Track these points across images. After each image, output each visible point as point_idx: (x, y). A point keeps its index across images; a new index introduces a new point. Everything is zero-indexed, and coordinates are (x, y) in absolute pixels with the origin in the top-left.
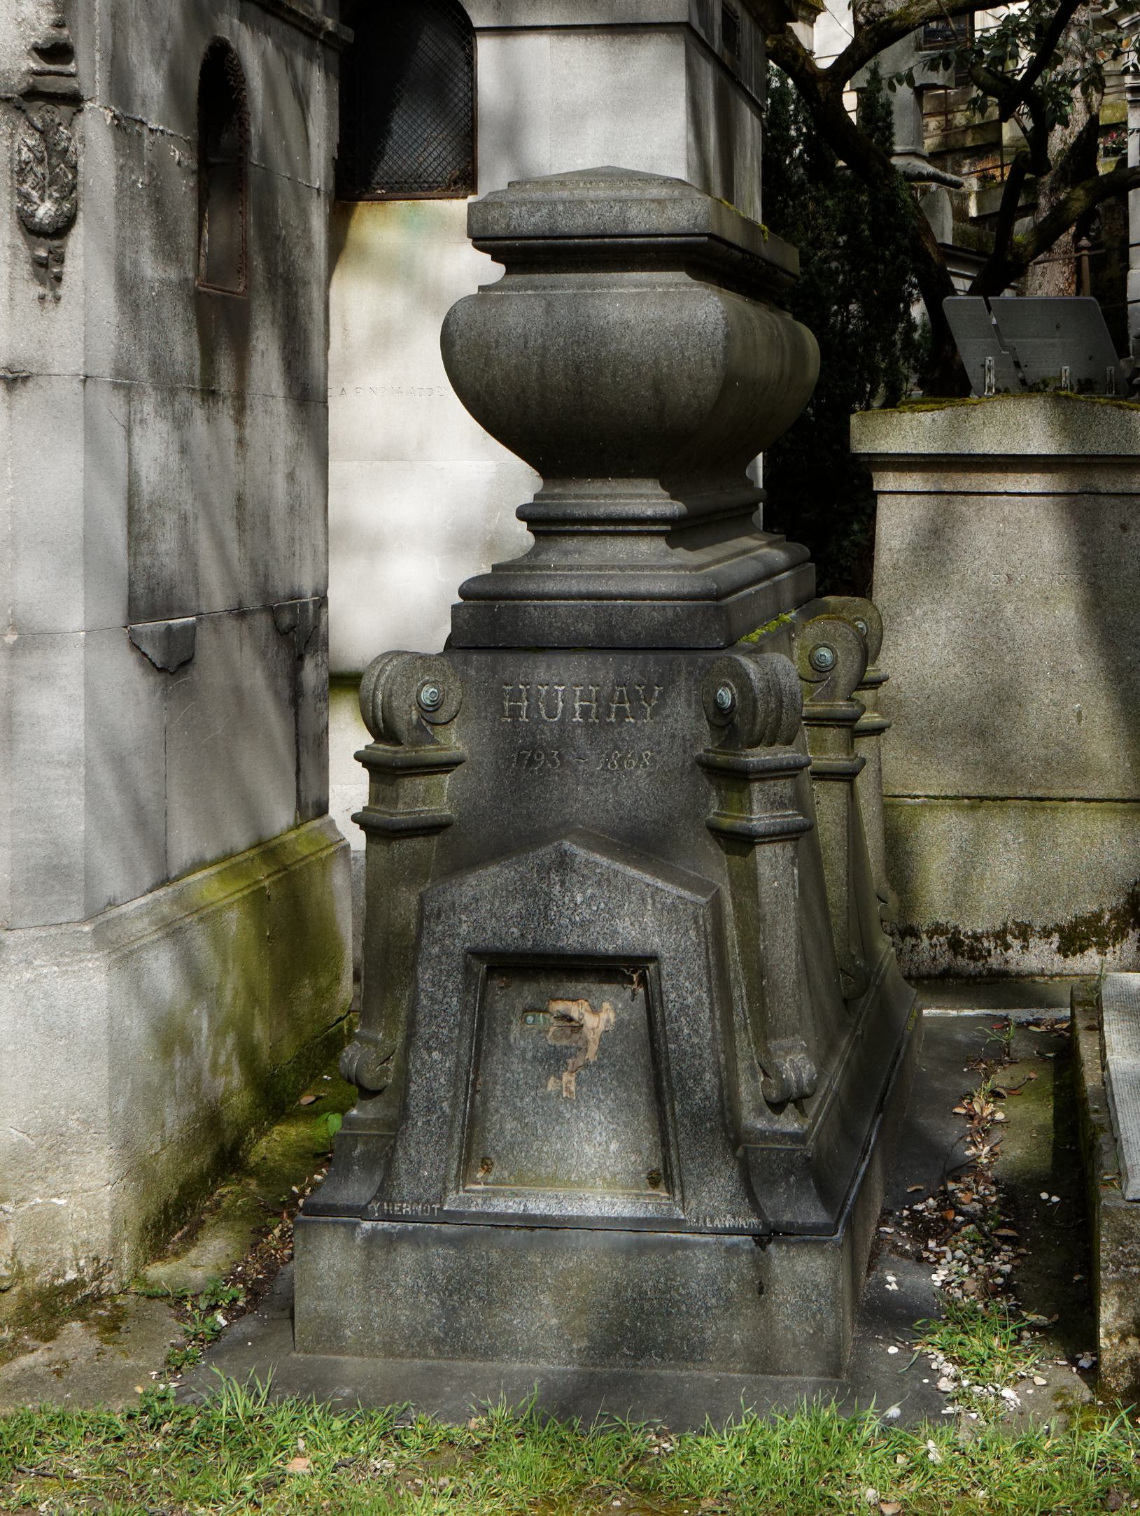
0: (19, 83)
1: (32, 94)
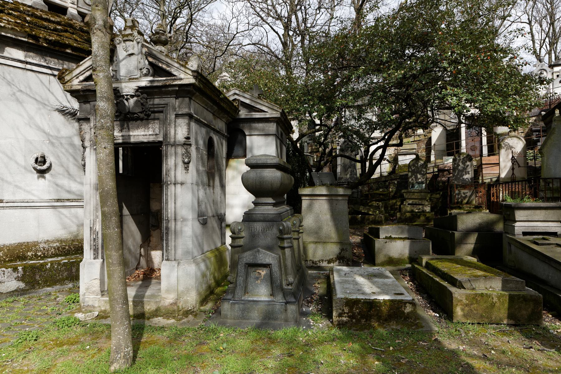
0: (183, 142)
1: (184, 144)
